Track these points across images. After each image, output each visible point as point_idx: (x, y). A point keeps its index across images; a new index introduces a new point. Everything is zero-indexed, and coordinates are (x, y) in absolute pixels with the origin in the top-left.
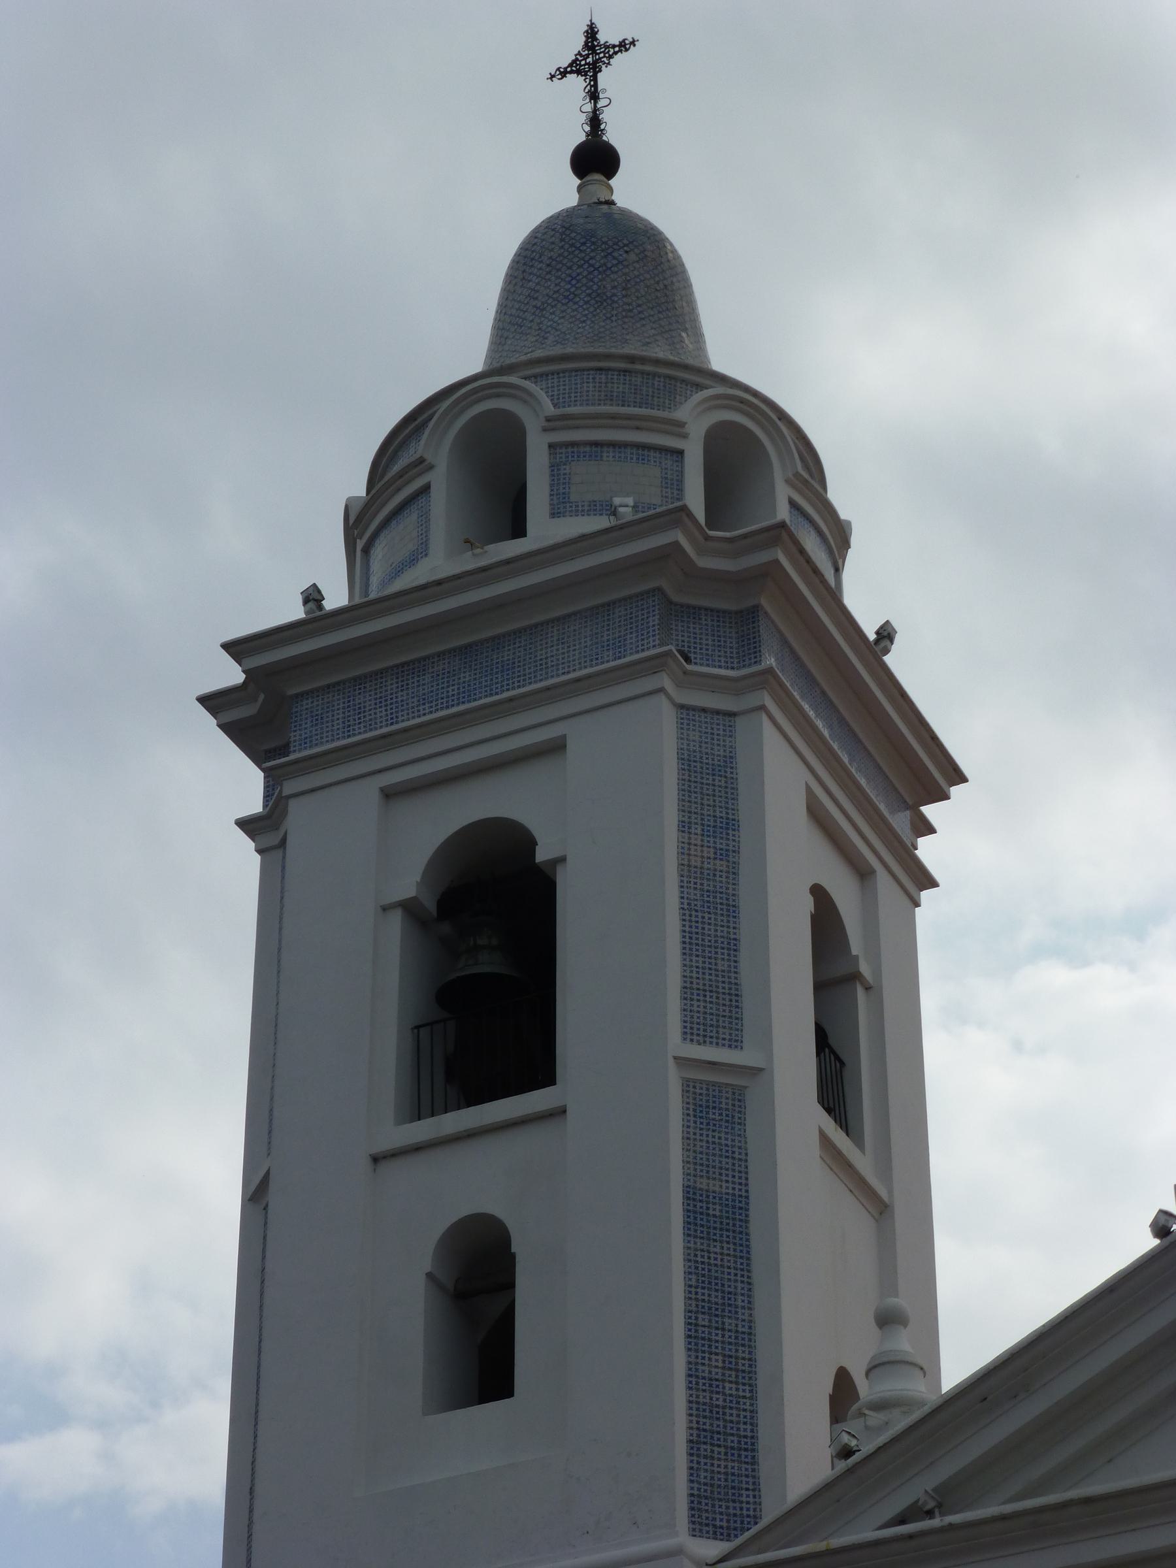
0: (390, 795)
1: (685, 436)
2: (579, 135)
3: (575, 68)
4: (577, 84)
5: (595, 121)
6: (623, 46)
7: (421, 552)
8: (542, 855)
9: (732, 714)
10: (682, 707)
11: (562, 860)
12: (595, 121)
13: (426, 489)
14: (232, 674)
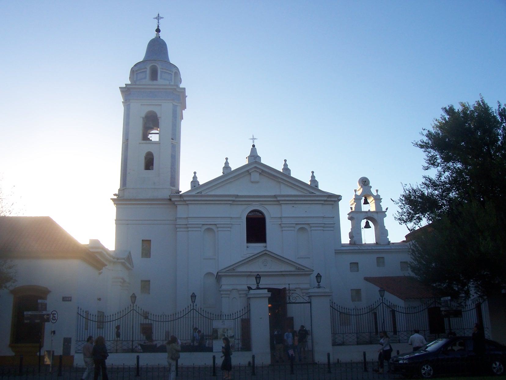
0: (141, 105)
1: (173, 73)
2: (156, 28)
3: (156, 18)
4: (156, 20)
5: (158, 26)
6: (162, 18)
7: (145, 78)
8: (158, 116)
9: (177, 106)
10: (173, 104)
11: (161, 117)
12: (158, 26)
13: (146, 71)
14: (125, 86)
